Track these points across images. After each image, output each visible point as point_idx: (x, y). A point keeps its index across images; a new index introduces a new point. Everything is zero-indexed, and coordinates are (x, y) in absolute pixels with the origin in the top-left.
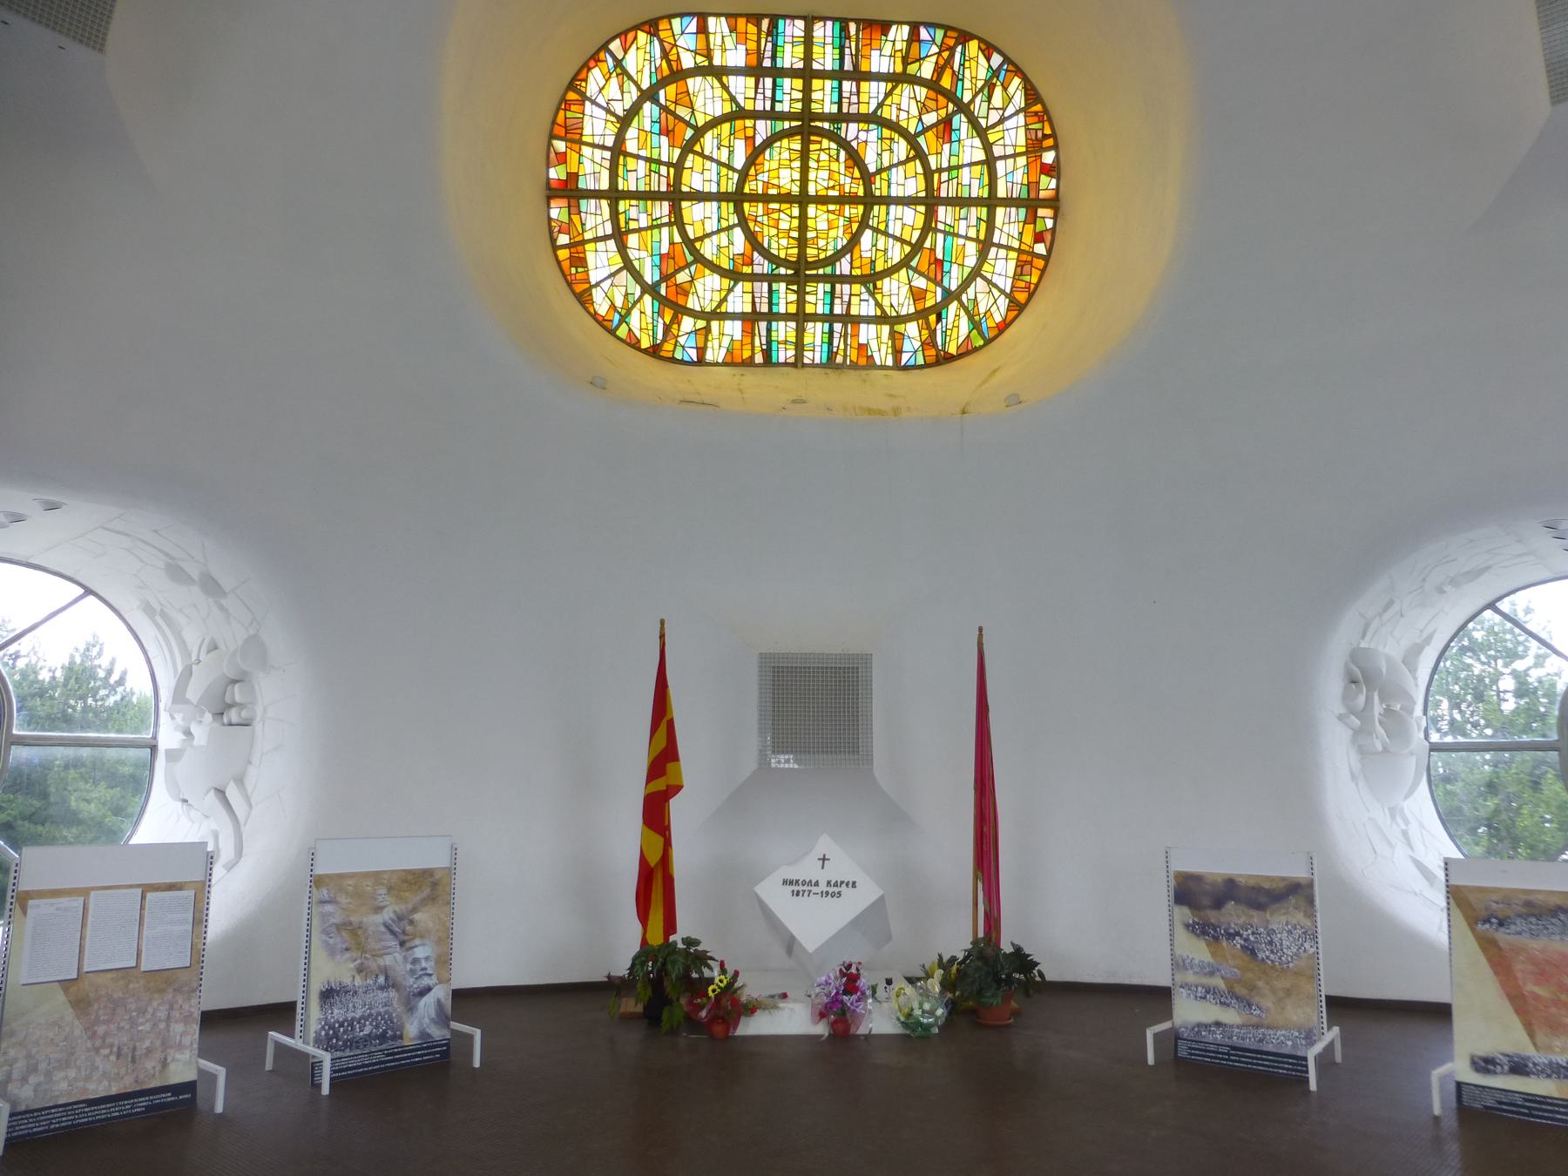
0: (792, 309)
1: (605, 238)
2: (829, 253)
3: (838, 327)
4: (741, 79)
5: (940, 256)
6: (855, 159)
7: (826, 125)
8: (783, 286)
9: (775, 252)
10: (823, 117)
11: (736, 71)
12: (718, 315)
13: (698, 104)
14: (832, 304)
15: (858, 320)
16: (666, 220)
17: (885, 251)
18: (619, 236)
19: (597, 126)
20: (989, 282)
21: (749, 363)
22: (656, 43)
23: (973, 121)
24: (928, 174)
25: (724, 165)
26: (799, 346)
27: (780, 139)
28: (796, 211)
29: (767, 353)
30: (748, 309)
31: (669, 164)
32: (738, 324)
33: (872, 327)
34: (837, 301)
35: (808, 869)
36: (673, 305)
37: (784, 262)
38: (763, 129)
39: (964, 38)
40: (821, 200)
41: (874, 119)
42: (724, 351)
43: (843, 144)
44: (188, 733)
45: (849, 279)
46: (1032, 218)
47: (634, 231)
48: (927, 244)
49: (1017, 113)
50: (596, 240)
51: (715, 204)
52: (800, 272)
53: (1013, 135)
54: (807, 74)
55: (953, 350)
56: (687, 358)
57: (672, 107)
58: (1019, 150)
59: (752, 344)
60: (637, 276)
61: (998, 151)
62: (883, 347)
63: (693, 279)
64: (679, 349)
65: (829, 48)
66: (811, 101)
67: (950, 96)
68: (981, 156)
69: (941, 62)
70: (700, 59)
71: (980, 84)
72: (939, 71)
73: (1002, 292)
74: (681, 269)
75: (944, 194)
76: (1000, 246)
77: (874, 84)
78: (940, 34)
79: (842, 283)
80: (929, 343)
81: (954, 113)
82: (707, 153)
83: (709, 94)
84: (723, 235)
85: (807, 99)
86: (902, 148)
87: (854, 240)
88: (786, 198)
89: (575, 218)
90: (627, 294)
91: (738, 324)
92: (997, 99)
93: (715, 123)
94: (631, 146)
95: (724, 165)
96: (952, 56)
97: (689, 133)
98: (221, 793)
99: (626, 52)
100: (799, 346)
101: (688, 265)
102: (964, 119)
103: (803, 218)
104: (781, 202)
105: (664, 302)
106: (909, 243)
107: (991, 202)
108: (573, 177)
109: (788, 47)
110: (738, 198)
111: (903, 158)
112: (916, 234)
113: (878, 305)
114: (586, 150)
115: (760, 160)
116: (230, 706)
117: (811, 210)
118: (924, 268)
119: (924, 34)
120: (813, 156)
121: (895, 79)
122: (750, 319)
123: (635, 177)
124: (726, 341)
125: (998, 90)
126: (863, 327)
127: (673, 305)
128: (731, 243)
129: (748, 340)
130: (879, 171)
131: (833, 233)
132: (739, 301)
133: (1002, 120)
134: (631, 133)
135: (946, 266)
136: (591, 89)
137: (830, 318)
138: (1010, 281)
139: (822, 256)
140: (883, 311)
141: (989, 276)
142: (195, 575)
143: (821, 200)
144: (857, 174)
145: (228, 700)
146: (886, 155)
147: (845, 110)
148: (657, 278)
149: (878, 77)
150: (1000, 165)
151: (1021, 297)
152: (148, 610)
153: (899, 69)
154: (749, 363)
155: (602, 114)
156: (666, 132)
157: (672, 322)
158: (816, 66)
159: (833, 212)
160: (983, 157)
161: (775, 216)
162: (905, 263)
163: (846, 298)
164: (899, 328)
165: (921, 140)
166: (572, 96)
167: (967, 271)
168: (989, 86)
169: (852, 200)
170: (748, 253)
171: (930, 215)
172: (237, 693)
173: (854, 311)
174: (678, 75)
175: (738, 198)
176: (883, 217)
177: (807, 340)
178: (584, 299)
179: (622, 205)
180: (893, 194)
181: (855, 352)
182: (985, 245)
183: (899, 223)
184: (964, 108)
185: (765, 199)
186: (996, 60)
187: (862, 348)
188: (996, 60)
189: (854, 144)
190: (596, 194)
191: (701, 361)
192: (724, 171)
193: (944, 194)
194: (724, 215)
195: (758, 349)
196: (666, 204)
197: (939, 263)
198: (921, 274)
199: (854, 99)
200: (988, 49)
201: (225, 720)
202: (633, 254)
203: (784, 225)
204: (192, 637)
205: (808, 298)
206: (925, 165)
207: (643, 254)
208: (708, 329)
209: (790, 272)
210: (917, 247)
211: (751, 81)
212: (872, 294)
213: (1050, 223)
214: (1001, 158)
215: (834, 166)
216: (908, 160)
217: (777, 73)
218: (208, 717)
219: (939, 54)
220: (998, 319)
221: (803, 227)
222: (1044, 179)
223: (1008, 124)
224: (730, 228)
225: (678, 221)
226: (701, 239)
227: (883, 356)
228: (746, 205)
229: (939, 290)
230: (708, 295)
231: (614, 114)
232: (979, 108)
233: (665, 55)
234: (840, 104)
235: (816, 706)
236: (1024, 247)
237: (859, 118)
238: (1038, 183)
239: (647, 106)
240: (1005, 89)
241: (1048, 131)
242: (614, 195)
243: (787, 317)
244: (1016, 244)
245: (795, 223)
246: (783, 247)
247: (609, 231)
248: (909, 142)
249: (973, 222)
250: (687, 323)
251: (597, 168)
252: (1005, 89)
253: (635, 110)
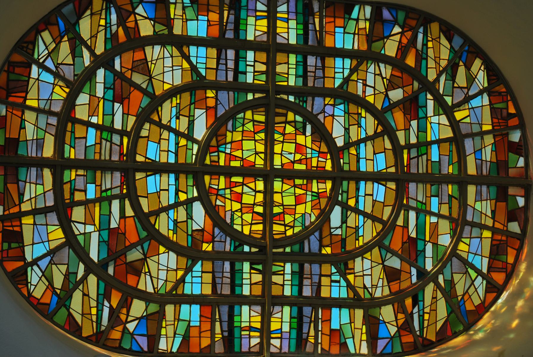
0: (258, 291)
1: (45, 211)
2: (297, 230)
3: (307, 310)
4: (202, 50)
5: (414, 235)
6: (322, 134)
7: (292, 98)
8: (246, 266)
9: (239, 228)
10: (289, 90)
11: (198, 42)
13: (156, 70)
14: (301, 286)
16: (117, 191)
17: (357, 228)
18: (62, 210)
19: (44, 88)
20: (465, 263)
22: (113, 10)
24: (397, 150)
25: (183, 135)
26: (265, 331)
27: (244, 111)
28: (260, 185)
30: (208, 290)
31: (122, 133)
32: (196, 308)
33: (345, 312)
34: (306, 282)
37: (249, 240)
39: (425, 19)
41: (343, 95)
42: (178, 341)
43: (310, 118)
46: (502, 196)
47: (80, 203)
48: (400, 222)
49: (480, 93)
50: (34, 212)
51: (172, 176)
52: (265, 253)
53: (478, 113)
54: (271, 47)
55: (432, 337)
56: (135, 348)
57: (128, 74)
58: (486, 128)
59: (212, 330)
60: (82, 254)
61: (464, 130)
62: (357, 333)
63: (144, 260)
64: (127, 337)
65: (293, 24)
66: (275, 74)
67: (416, 74)
69: (405, 41)
70: (159, 27)
71: (444, 63)
72: (403, 50)
73: (479, 272)
74: (133, 246)
75: (413, 170)
76: (473, 225)
77: (339, 62)
78: (401, 16)
79: (311, 263)
80: (406, 327)
81: (420, 90)
82: (164, 122)
83: (168, 62)
84: (182, 210)
85: (271, 73)
86: (370, 124)
87: (324, 216)
88: (249, 172)
89: (12, 187)
90: (67, 276)
91: (196, 308)
93: (174, 92)
94: (81, 113)
95: (183, 135)
96: (416, 37)
97: (146, 101)
99: (80, 16)
100: (265, 331)
101: (141, 242)
102: (429, 96)
103: (268, 192)
104: (244, 175)
106: (380, 221)
109: (251, 20)
110: (196, 172)
111: (371, 132)
112: (388, 211)
113: (349, 286)
114: (30, 116)
115: (223, 129)
117: (277, 185)
118: (397, 246)
119: (386, 14)
120: (279, 128)
121: (360, 58)
124: (182, 328)
125: (462, 70)
126: (335, 311)
128: (190, 216)
129: (207, 326)
130: (348, 145)
131: (300, 209)
132: (198, 284)
133: (468, 99)
134: (83, 99)
135: (420, 246)
136: (41, 50)
138: (486, 261)
139: (289, 233)
140: (356, 293)
141: (464, 255)
143: (287, 174)
144: (324, 149)
146: (353, 130)
147: (310, 84)
148: (104, 255)
149: (343, 53)
150: (468, 144)
151: (499, 277)
153: (364, 47)
155: (49, 78)
157: (121, 305)
158: (279, 40)
159: (300, 187)
160: (451, 135)
161: (238, 189)
162: (378, 242)
163: (316, 279)
164: (374, 312)
165: (388, 116)
166: (17, 58)
167: (441, 250)
168: (451, 70)
169: (320, 175)
170: (209, 228)
171: (401, 192)
173: (325, 293)
174: (137, 42)
175: (196, 172)
176: (352, 192)
177: (274, 326)
178: (19, 278)
179: (70, 175)
180: (363, 169)
181: (326, 339)
182: (460, 225)
183: (369, 199)
184: (430, 87)
185: (228, 172)
186: (458, 41)
187: (336, 335)
188: (458, 41)
189: (321, 117)
190: (41, 163)
192: (183, 142)
193: (413, 170)
194: (182, 187)
195: (218, 337)
196: (117, 175)
197: (413, 242)
198: (394, 253)
199: (319, 73)
200: (449, 31)
202: (79, 229)
203: (247, 199)
205: (275, 279)
206: (394, 140)
207: (90, 228)
208: (161, 314)
209: (254, 250)
210: (389, 227)
211: (213, 52)
212: (344, 275)
213: (521, 202)
214: (468, 136)
215: (300, 139)
216: (376, 135)
217: (242, 45)
219: (402, 33)
220: (477, 302)
221: (268, 203)
222: (512, 156)
223: (475, 102)
224: (189, 202)
225: (131, 195)
226: (157, 213)
228: (207, 178)
229: (414, 271)
230: (163, 275)
231: (63, 79)
233: (122, 22)
234: (305, 76)
236: (497, 225)
237: (325, 93)
238: (506, 162)
239: (101, 73)
240: (468, 67)
241: (512, 110)
242: (59, 165)
244: (489, 222)
245: (260, 197)
247: (50, 203)
248: (375, 117)
249: (446, 199)
250: (138, 308)
251: (41, 134)
252: (468, 67)
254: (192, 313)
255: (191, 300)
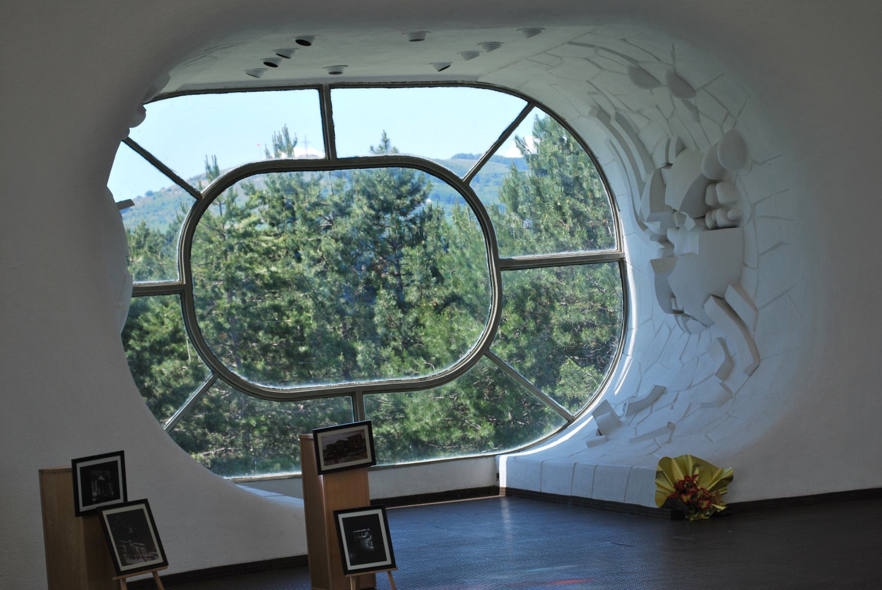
44: (664, 240)
98: (720, 299)
116: (710, 209)
142: (661, 75)
145: (709, 201)
152: (602, 115)
172: (720, 193)
201: (709, 223)
204: (654, 137)
218: (690, 223)
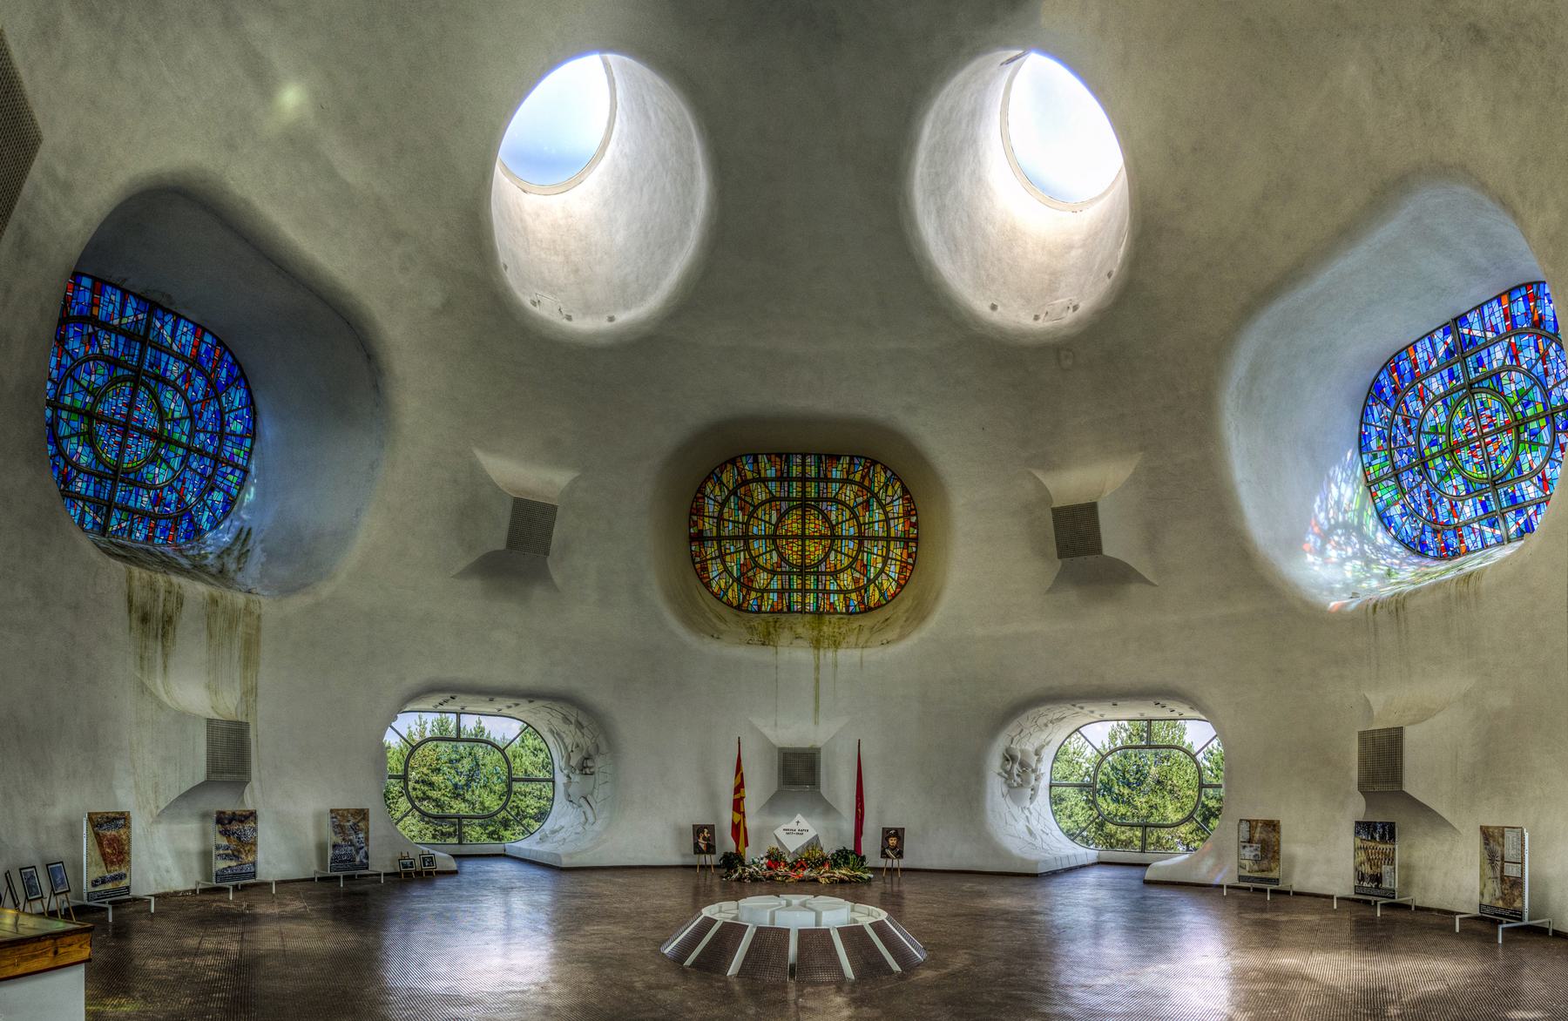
6: (826, 519)
12: (766, 590)
15: (830, 592)
19: (711, 508)
21: (781, 611)
23: (879, 501)
24: (859, 525)
29: (789, 607)
35: (792, 825)
36: (745, 584)
38: (784, 505)
40: (812, 538)
43: (821, 511)
45: (826, 574)
52: (803, 570)
53: (898, 508)
60: (731, 574)
68: (882, 517)
86: (847, 514)
87: (827, 555)
88: (795, 537)
92: (890, 492)
94: (726, 516)
100: (803, 604)
103: (803, 545)
105: (743, 585)
107: (888, 539)
108: (701, 531)
110: (773, 538)
122: (781, 592)
123: (729, 529)
127: (745, 584)
132: (775, 585)
137: (817, 591)
143: (812, 538)
154: (781, 611)
156: (741, 509)
162: (850, 566)
171: (861, 544)
175: (773, 538)
184: (875, 496)
185: (786, 537)
190: (711, 539)
191: (759, 611)
210: (855, 559)
225: (747, 549)
227: (840, 607)
232: (882, 495)
235: (799, 772)
243: (797, 591)
246: (794, 558)
250: (753, 595)
253: (727, 499)
254: (773, 596)
255: (773, 591)
